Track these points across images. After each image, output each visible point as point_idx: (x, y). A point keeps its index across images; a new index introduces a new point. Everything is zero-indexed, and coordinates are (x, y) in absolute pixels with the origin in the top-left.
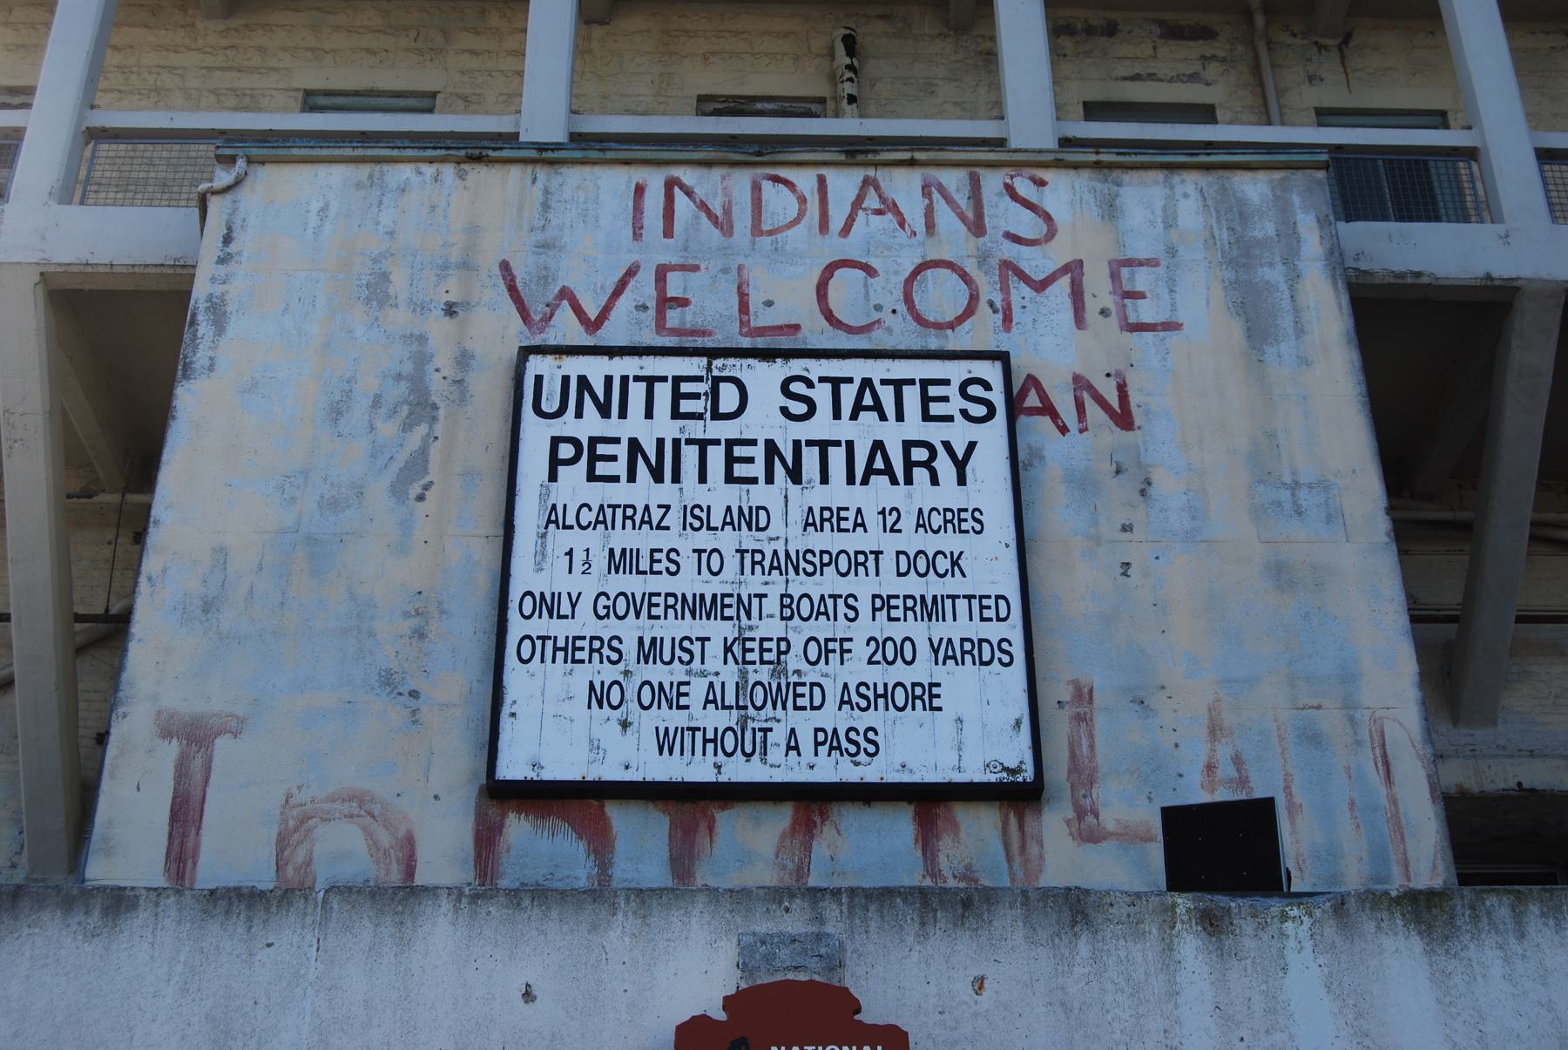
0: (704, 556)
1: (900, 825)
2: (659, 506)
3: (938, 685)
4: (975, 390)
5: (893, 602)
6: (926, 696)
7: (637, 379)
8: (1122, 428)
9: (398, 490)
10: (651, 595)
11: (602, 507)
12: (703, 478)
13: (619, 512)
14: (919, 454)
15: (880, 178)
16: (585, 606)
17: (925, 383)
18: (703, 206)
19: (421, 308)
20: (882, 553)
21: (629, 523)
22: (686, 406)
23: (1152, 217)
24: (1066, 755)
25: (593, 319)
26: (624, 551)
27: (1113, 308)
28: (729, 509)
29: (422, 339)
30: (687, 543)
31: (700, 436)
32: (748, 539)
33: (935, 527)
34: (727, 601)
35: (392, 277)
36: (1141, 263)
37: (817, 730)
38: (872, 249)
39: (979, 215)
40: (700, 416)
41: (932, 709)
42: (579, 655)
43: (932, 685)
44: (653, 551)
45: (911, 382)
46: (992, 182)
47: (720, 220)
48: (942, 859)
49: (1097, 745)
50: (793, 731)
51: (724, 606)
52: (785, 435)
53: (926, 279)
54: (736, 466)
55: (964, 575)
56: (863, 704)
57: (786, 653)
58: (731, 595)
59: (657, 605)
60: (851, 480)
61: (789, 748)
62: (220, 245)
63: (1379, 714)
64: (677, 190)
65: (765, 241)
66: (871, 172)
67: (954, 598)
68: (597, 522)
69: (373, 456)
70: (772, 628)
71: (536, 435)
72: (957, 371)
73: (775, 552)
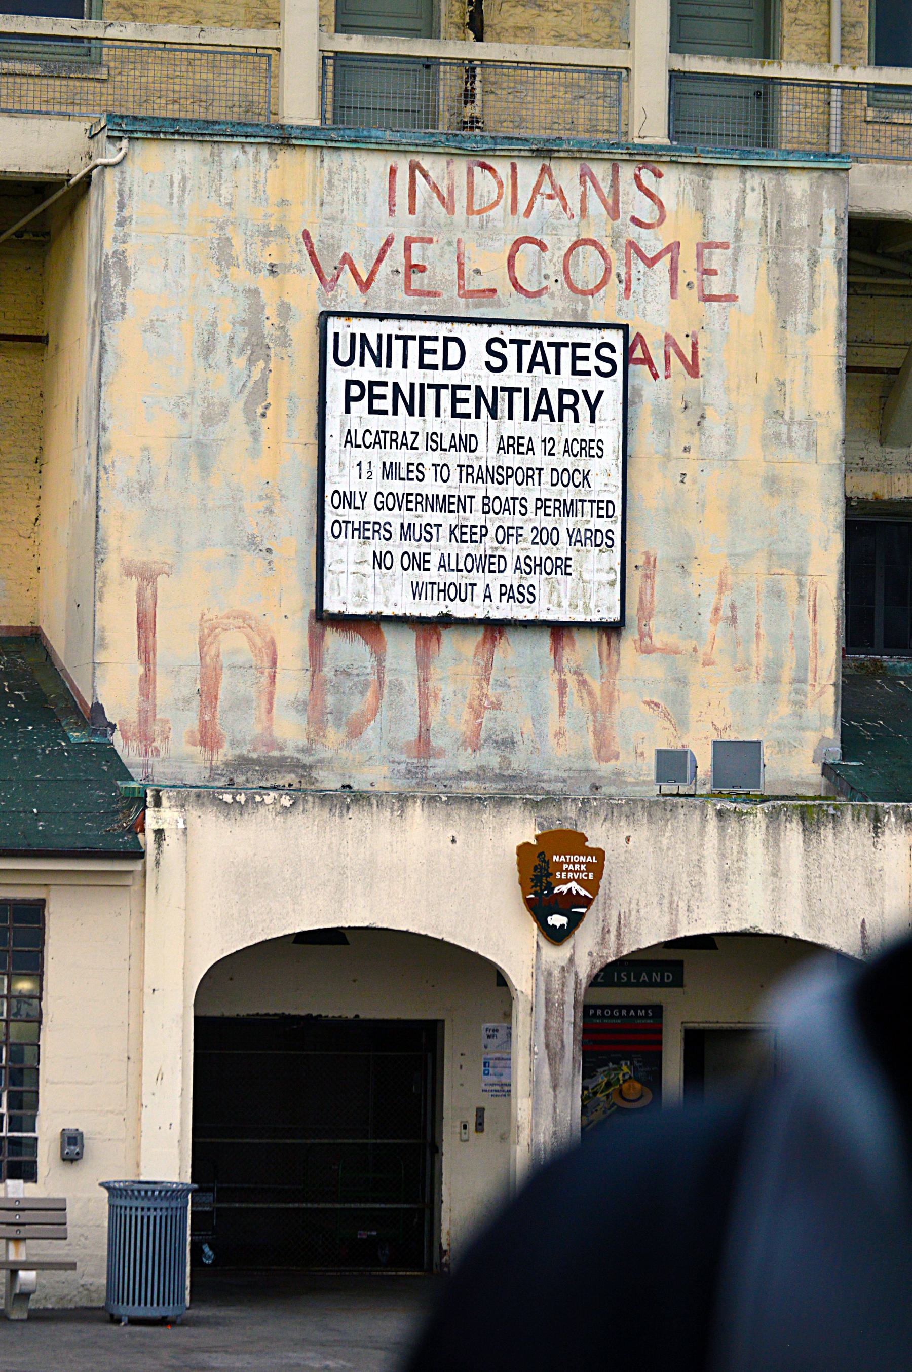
0: (439, 469)
1: (545, 641)
2: (412, 433)
3: (570, 559)
4: (605, 352)
5: (548, 503)
6: (563, 566)
7: (397, 337)
8: (692, 376)
9: (248, 410)
10: (408, 494)
11: (378, 432)
12: (438, 414)
13: (388, 436)
14: (568, 399)
15: (552, 167)
16: (370, 500)
17: (575, 346)
18: (435, 187)
19: (255, 268)
20: (542, 469)
21: (394, 444)
22: (428, 359)
23: (728, 207)
24: (638, 599)
25: (364, 280)
26: (391, 463)
27: (696, 283)
28: (453, 436)
29: (255, 293)
30: (430, 458)
31: (436, 382)
32: (464, 457)
33: (575, 453)
34: (452, 500)
35: (233, 242)
36: (718, 246)
37: (501, 586)
38: (544, 228)
39: (616, 202)
40: (435, 367)
41: (567, 574)
42: (367, 534)
43: (567, 559)
44: (409, 464)
45: (566, 345)
46: (627, 172)
47: (446, 200)
48: (564, 660)
49: (655, 594)
50: (488, 585)
51: (450, 503)
52: (489, 381)
53: (578, 253)
54: (458, 405)
55: (590, 486)
56: (528, 570)
57: (485, 535)
58: (454, 496)
59: (411, 502)
60: (526, 418)
61: (486, 597)
62: (116, 210)
63: (816, 579)
64: (417, 172)
65: (476, 218)
66: (547, 162)
67: (582, 501)
68: (375, 443)
69: (232, 383)
70: (476, 518)
71: (336, 377)
72: (594, 337)
73: (480, 467)
